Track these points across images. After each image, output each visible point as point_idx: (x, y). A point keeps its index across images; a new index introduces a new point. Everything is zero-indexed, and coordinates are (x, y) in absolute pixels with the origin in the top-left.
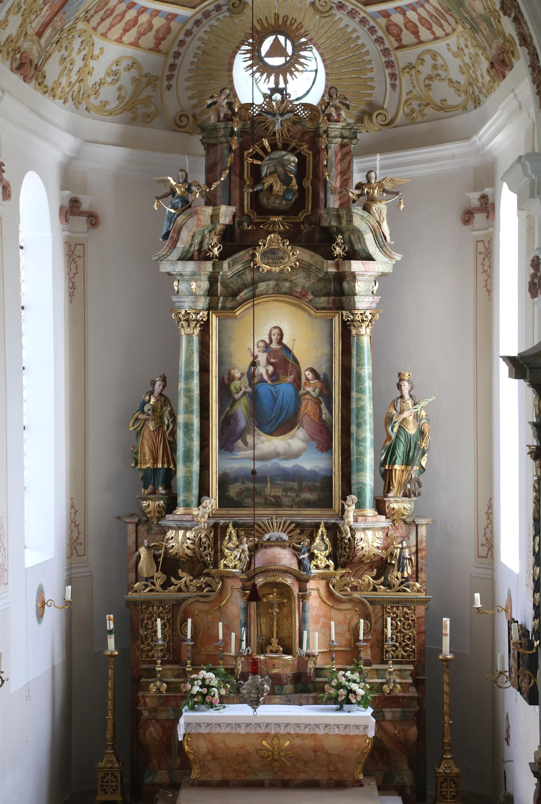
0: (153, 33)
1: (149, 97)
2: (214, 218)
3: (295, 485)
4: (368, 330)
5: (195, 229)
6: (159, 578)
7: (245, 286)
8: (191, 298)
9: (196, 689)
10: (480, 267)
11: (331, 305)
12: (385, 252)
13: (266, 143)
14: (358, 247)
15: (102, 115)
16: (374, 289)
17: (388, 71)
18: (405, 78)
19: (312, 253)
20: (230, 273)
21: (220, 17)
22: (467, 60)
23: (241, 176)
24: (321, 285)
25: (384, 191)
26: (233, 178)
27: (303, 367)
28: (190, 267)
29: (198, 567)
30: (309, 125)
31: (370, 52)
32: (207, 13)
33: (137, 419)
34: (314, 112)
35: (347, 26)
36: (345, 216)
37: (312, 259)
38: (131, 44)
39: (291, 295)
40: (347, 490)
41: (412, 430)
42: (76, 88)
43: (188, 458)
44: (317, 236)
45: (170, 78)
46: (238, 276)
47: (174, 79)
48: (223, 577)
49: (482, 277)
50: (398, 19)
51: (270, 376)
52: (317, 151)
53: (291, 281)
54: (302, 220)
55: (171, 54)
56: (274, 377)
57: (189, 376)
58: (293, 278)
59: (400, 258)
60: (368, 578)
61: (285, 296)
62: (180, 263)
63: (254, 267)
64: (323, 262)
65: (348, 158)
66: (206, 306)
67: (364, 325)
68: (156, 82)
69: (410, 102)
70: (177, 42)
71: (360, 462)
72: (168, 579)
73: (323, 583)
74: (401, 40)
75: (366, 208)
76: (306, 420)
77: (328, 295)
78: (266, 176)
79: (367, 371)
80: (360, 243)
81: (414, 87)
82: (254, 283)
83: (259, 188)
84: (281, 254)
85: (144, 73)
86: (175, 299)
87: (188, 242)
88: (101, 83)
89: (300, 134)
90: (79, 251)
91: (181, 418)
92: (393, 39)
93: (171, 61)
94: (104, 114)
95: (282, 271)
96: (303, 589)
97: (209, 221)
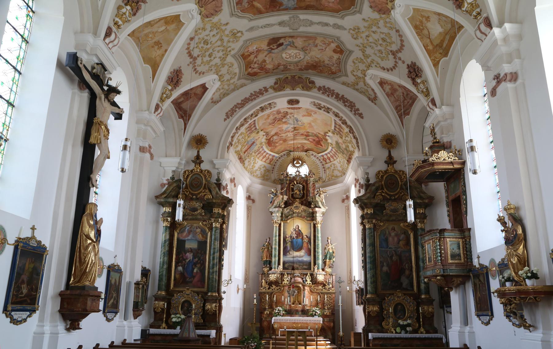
0: (269, 160)
1: (268, 175)
2: (283, 199)
3: (302, 264)
5: (278, 201)
6: (267, 287)
7: (290, 215)
8: (277, 217)
9: (277, 311)
10: (347, 213)
13: (295, 182)
14: (317, 205)
18: (327, 171)
22: (342, 164)
23: (289, 190)
24: (308, 215)
25: (323, 192)
27: (304, 235)
28: (277, 209)
30: (305, 179)
33: (262, 249)
38: (264, 162)
40: (315, 264)
41: (331, 251)
42: (251, 170)
43: (275, 256)
44: (307, 204)
45: (273, 171)
48: (283, 286)
49: (347, 215)
50: (325, 157)
51: (296, 237)
52: (307, 184)
56: (297, 237)
57: (276, 236)
60: (320, 287)
71: (318, 258)
72: (270, 287)
73: (309, 288)
75: (319, 196)
76: (305, 248)
77: (310, 217)
79: (320, 235)
86: (273, 218)
88: (257, 170)
91: (274, 247)
95: (299, 212)
96: (304, 288)
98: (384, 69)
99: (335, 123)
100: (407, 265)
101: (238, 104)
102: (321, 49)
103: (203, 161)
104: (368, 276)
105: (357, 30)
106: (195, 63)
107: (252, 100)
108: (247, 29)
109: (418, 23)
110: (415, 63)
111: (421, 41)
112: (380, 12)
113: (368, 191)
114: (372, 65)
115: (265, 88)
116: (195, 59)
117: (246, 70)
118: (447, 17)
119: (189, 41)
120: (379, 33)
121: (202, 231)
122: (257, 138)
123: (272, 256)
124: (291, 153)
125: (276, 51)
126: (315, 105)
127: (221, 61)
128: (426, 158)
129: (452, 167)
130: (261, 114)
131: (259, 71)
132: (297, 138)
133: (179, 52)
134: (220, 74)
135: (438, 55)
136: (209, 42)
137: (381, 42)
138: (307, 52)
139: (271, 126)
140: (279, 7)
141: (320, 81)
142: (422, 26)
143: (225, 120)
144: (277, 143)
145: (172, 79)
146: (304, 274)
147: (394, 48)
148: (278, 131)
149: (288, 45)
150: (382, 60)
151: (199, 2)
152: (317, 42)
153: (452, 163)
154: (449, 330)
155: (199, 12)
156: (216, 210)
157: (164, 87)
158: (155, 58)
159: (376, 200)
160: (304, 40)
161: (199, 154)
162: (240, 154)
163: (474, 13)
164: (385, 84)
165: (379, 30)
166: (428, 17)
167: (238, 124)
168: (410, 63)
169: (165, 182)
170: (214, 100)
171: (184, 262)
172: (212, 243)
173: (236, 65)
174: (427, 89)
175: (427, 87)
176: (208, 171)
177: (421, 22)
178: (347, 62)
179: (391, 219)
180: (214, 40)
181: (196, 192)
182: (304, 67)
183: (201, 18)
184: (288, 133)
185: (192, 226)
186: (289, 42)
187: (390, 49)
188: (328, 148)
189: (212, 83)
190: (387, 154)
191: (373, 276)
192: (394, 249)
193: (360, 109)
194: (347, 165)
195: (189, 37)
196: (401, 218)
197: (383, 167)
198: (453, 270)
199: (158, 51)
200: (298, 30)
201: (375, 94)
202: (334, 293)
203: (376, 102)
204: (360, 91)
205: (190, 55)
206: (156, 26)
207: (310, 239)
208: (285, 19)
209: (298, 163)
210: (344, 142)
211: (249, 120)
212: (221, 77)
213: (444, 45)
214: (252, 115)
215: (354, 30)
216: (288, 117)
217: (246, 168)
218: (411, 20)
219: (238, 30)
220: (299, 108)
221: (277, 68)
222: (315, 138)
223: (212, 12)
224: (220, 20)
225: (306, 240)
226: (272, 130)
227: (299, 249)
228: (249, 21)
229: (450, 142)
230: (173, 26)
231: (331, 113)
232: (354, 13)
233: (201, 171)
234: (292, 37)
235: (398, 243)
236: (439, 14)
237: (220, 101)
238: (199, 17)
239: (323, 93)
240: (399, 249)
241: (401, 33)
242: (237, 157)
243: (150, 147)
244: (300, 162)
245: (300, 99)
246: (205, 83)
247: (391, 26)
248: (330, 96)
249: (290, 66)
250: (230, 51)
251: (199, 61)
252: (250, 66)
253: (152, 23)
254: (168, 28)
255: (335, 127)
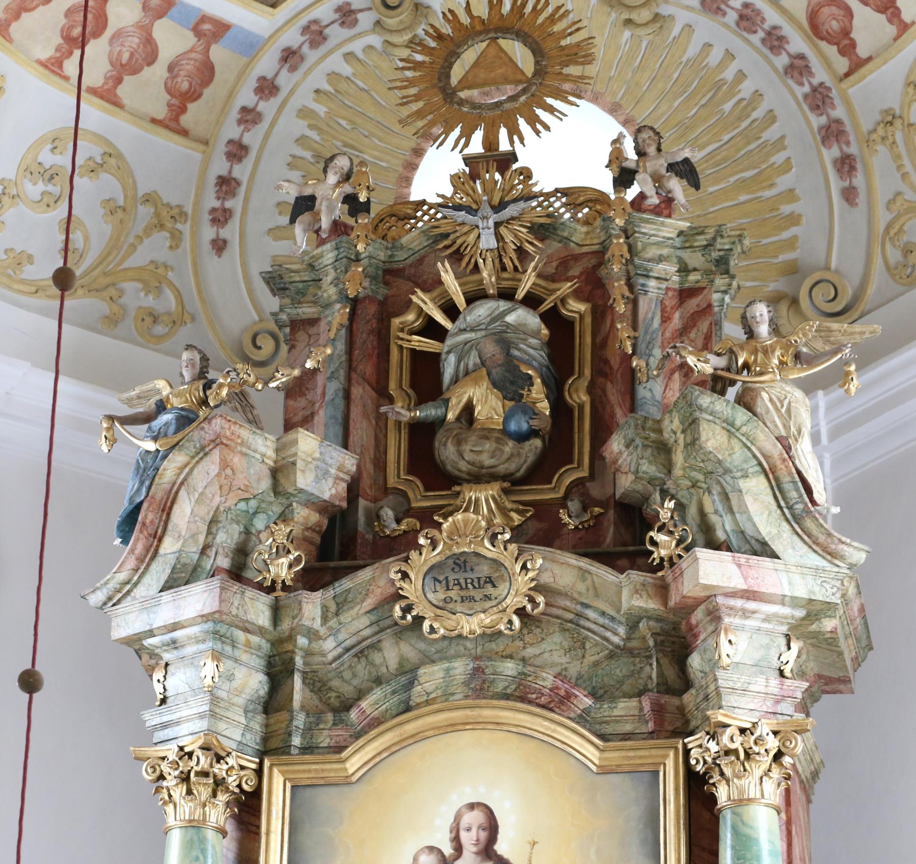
0: (157, 73)
4: (769, 786)
7: (378, 681)
11: (651, 726)
12: (809, 536)
13: (449, 278)
14: (723, 527)
15: (10, 288)
16: (784, 659)
17: (830, 154)
19: (584, 563)
20: (329, 645)
21: (357, 46)
26: (357, 392)
31: (776, 113)
32: (314, 27)
34: (598, 207)
35: (708, 45)
36: (681, 437)
37: (584, 580)
39: (523, 699)
45: (221, 217)
46: (360, 654)
47: (234, 224)
53: (523, 660)
54: (561, 493)
55: (221, 148)
58: (530, 651)
59: (863, 556)
61: (503, 703)
62: (167, 596)
63: (403, 617)
64: (620, 588)
65: (704, 326)
66: (253, 740)
67: (757, 769)
68: (179, 226)
69: (897, 227)
70: (234, 115)
74: (853, 44)
78: (456, 380)
80: (731, 510)
81: (904, 176)
83: (429, 412)
84: (484, 570)
85: (140, 193)
86: (152, 718)
87: (194, 536)
89: (554, 264)
92: (831, 51)
93: (220, 166)
94: (16, 286)
97: (265, 484)
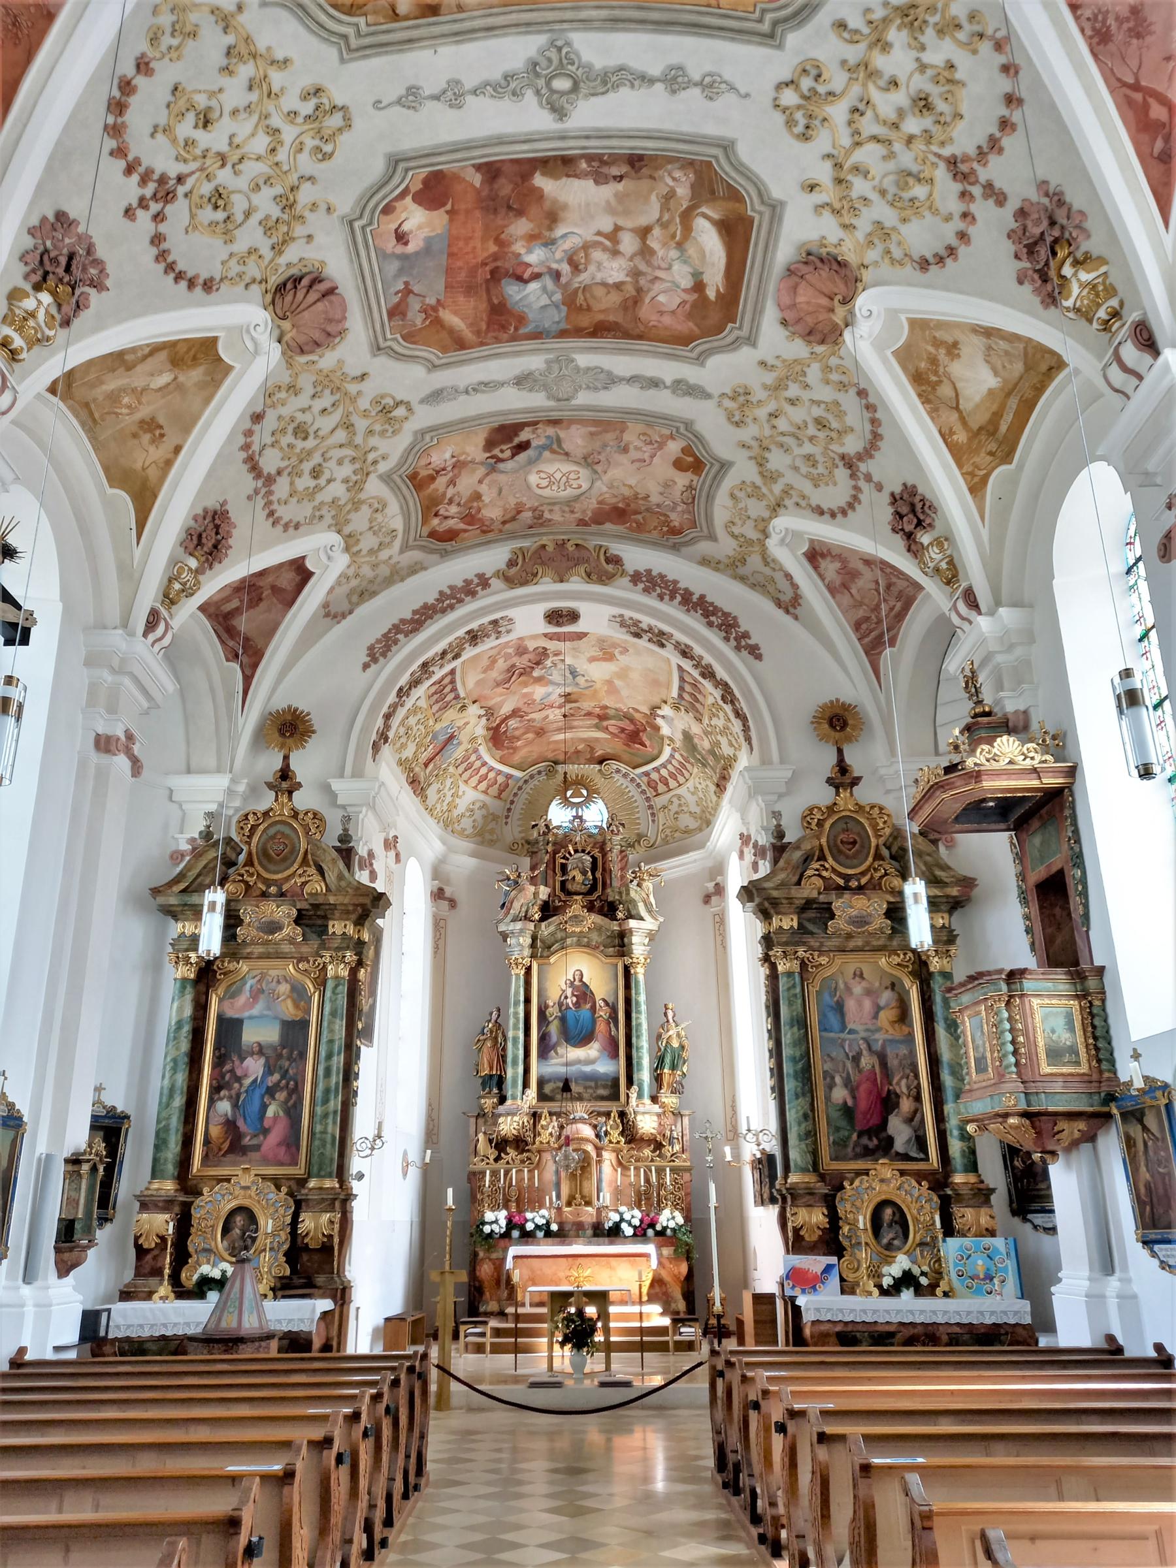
2: (536, 894)
6: (492, 1153)
14: (633, 912)
18: (661, 815)
22: (701, 795)
27: (598, 998)
28: (519, 925)
29: (522, 1145)
41: (675, 1044)
43: (515, 1063)
49: (719, 939)
50: (655, 776)
52: (604, 855)
56: (577, 1005)
57: (516, 1003)
60: (647, 1152)
71: (639, 1064)
75: (639, 885)
79: (642, 998)
82: (564, 939)
88: (463, 815)
90: (442, 923)
91: (510, 1034)
96: (599, 1155)
98: (822, 513)
99: (682, 679)
100: (904, 1082)
101: (403, 621)
102: (639, 460)
103: (299, 785)
104: (791, 1116)
105: (742, 399)
106: (270, 493)
107: (443, 611)
108: (422, 395)
109: (923, 365)
110: (914, 486)
111: (932, 419)
112: (811, 338)
113: (781, 863)
114: (787, 502)
115: (481, 576)
116: (270, 480)
117: (425, 521)
118: (1013, 338)
119: (248, 424)
120: (807, 403)
121: (294, 988)
122: (460, 723)
123: (505, 1062)
124: (560, 768)
125: (509, 465)
126: (623, 624)
127: (348, 490)
128: (956, 759)
129: (1035, 783)
130: (469, 653)
131: (462, 526)
132: (576, 723)
133: (219, 455)
134: (347, 530)
135: (983, 459)
136: (311, 431)
137: (812, 430)
138: (599, 468)
139: (500, 690)
140: (516, 329)
141: (637, 557)
142: (936, 373)
143: (366, 666)
144: (518, 739)
145: (200, 536)
146: (600, 1114)
147: (852, 445)
148: (520, 705)
149: (544, 448)
150: (816, 486)
151: (273, 302)
152: (627, 437)
153: (1035, 770)
154: (1053, 1289)
155: (276, 333)
156: (337, 927)
157: (173, 561)
158: (144, 469)
159: (811, 888)
160: (592, 434)
161: (288, 766)
162: (411, 770)
163: (1102, 314)
164: (823, 556)
165: (806, 395)
166: (955, 345)
167: (404, 680)
168: (898, 490)
169: (185, 847)
170: (333, 609)
171: (236, 1085)
172: (325, 1024)
173: (394, 507)
174: (951, 562)
175: (951, 556)
176: (315, 814)
177: (934, 361)
178: (713, 498)
179: (852, 944)
180: (326, 424)
181: (279, 876)
182: (589, 514)
183: (283, 353)
184: (549, 712)
185: (263, 976)
186: (548, 437)
187: (841, 450)
188: (660, 752)
189: (324, 558)
190: (833, 759)
191: (805, 1116)
192: (863, 1034)
193: (752, 634)
194: (714, 798)
195: (251, 412)
196: (880, 943)
197: (823, 795)
198: (1058, 1097)
199: (152, 449)
200: (574, 402)
201: (795, 586)
202: (688, 1170)
203: (798, 611)
204: (752, 580)
205: (254, 467)
206: (139, 368)
207: (614, 1010)
208: (533, 367)
209: (577, 794)
210: (706, 733)
211: (435, 669)
212: (350, 542)
213: (1003, 428)
214: (444, 653)
215: (733, 399)
216: (548, 663)
217: (431, 811)
218: (904, 356)
219: (399, 398)
220: (581, 636)
221: (513, 519)
222: (625, 724)
223: (317, 335)
224: (341, 362)
225: (603, 1013)
226: (503, 702)
227: (584, 1039)
228: (429, 371)
229: (1025, 712)
230: (196, 375)
231: (670, 647)
232: (734, 345)
233: (295, 814)
234: (555, 422)
235: (876, 1016)
236: (989, 333)
237: (351, 612)
238: (276, 350)
239: (646, 590)
240: (877, 1036)
241: (872, 400)
242: (403, 778)
243: (130, 737)
244: (585, 792)
245: (582, 607)
246: (303, 558)
247: (844, 379)
248: (667, 598)
249: (551, 511)
250: (375, 462)
251: (281, 488)
252: (434, 510)
253: (127, 357)
254: (181, 378)
255: (681, 689)
